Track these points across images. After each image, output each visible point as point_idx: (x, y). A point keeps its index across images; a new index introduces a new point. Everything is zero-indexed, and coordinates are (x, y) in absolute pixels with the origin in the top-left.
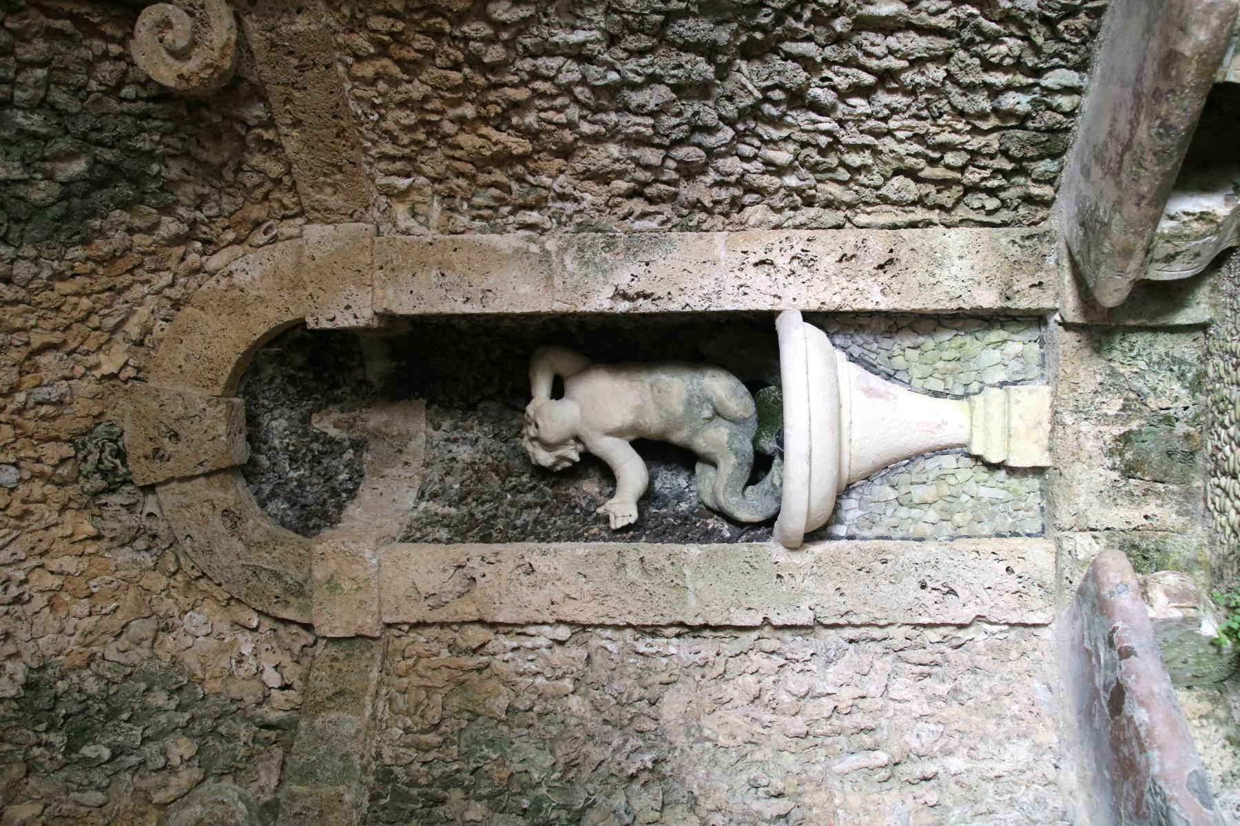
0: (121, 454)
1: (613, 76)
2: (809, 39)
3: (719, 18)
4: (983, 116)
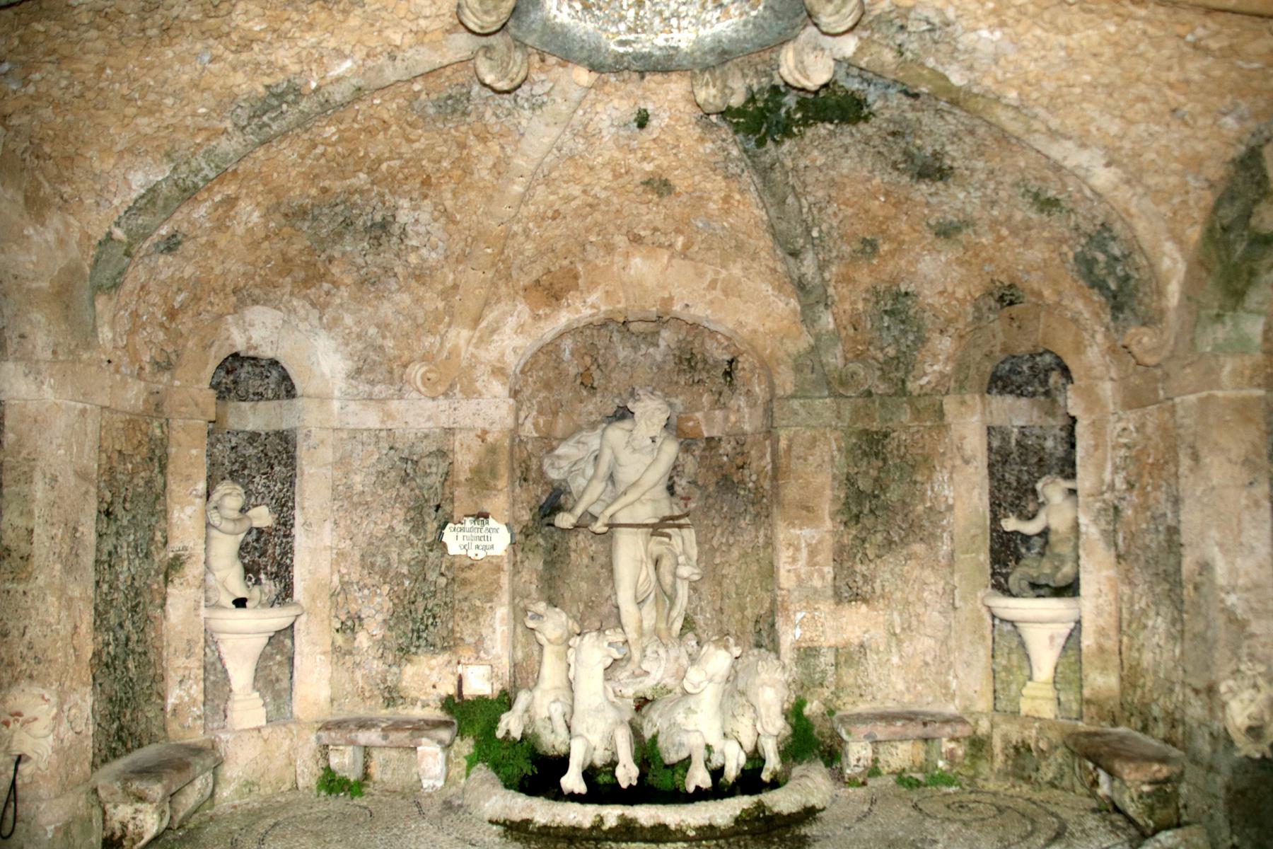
0: (1011, 303)
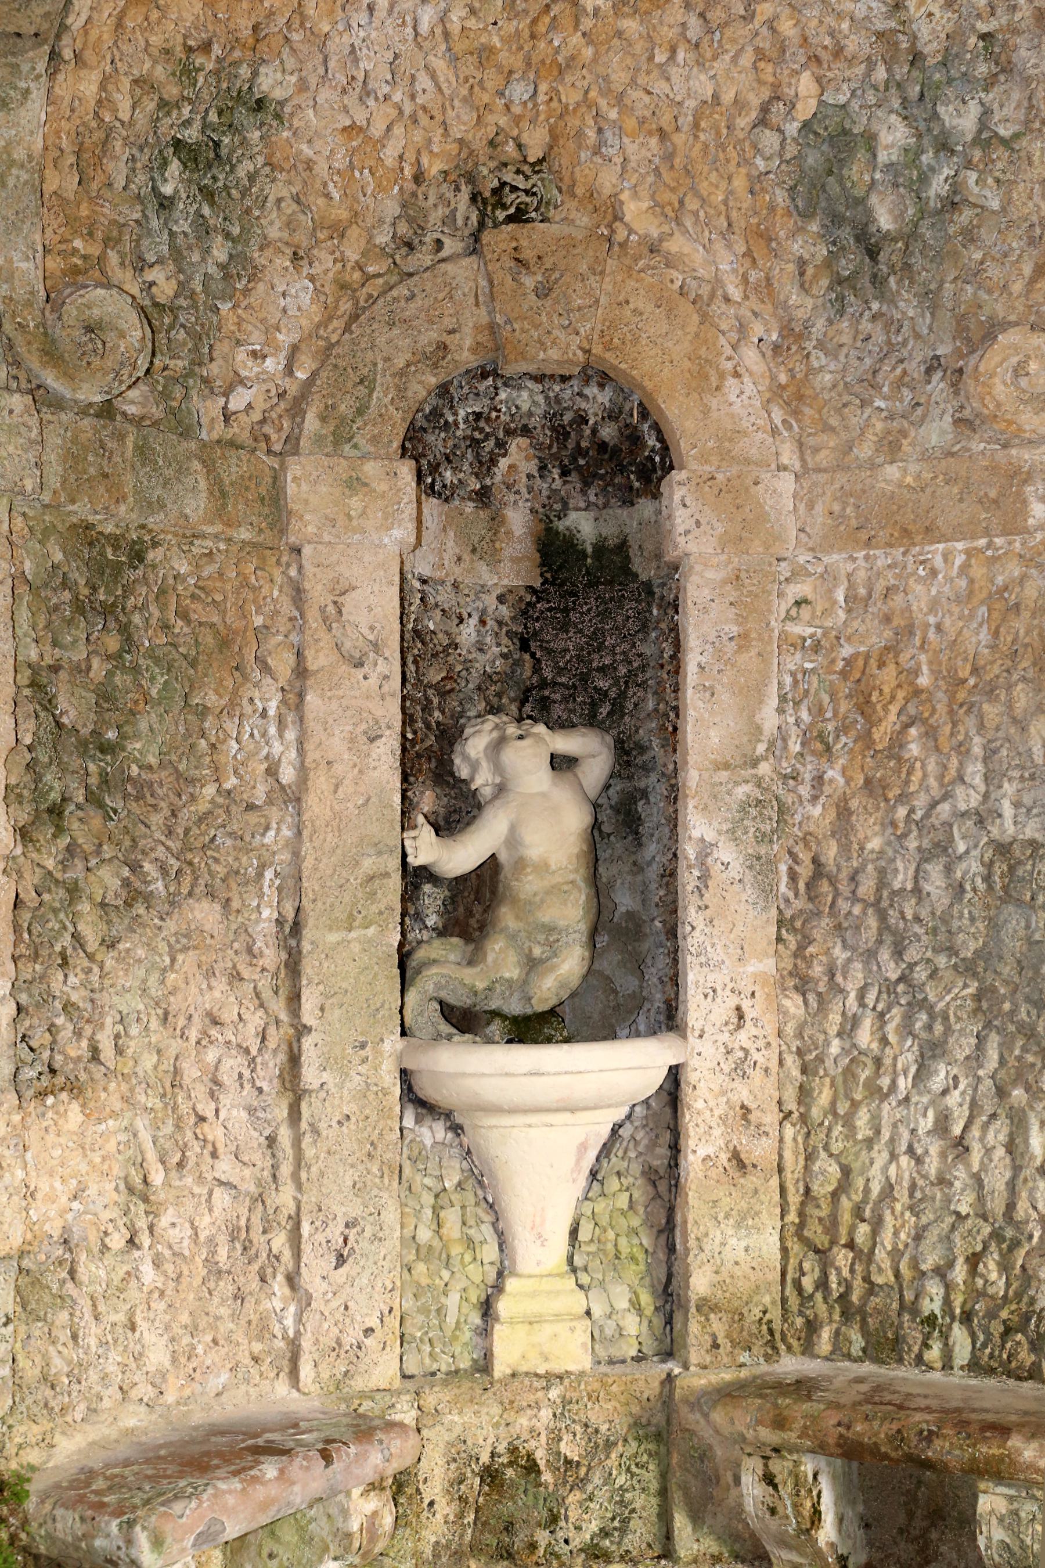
0: (519, 217)
1: (961, 848)
2: (1002, 1061)
3: (1025, 963)
4: (915, 1264)
